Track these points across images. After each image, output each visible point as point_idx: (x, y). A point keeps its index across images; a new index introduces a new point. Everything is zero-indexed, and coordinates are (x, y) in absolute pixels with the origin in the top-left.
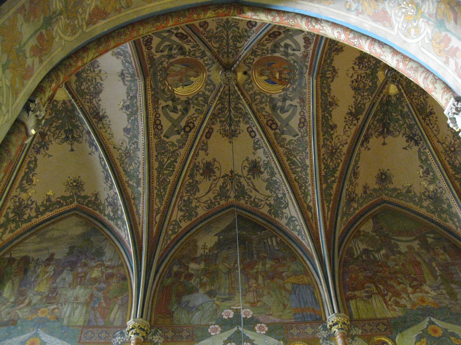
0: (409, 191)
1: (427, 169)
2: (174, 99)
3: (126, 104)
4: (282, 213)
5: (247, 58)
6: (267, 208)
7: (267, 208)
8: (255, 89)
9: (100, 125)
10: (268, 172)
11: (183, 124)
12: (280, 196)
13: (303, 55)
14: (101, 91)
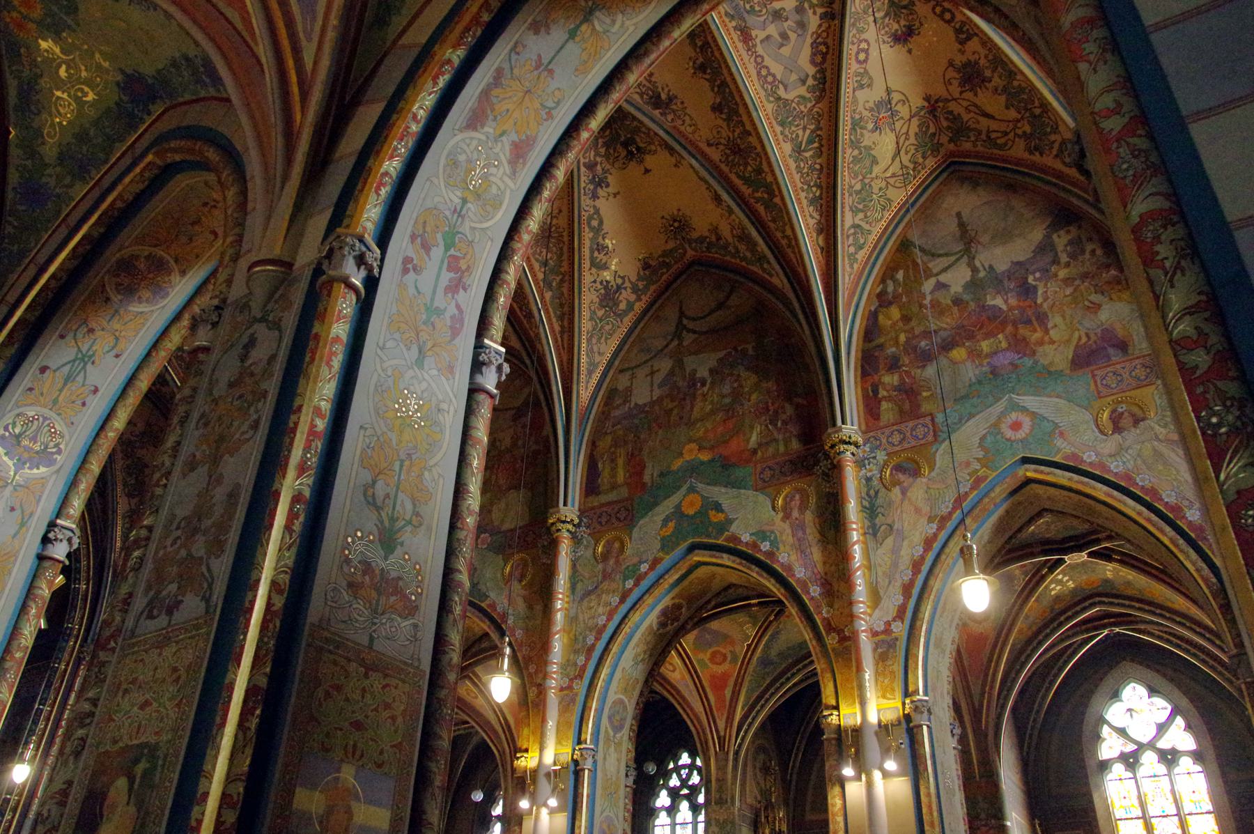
3: (698, 62)
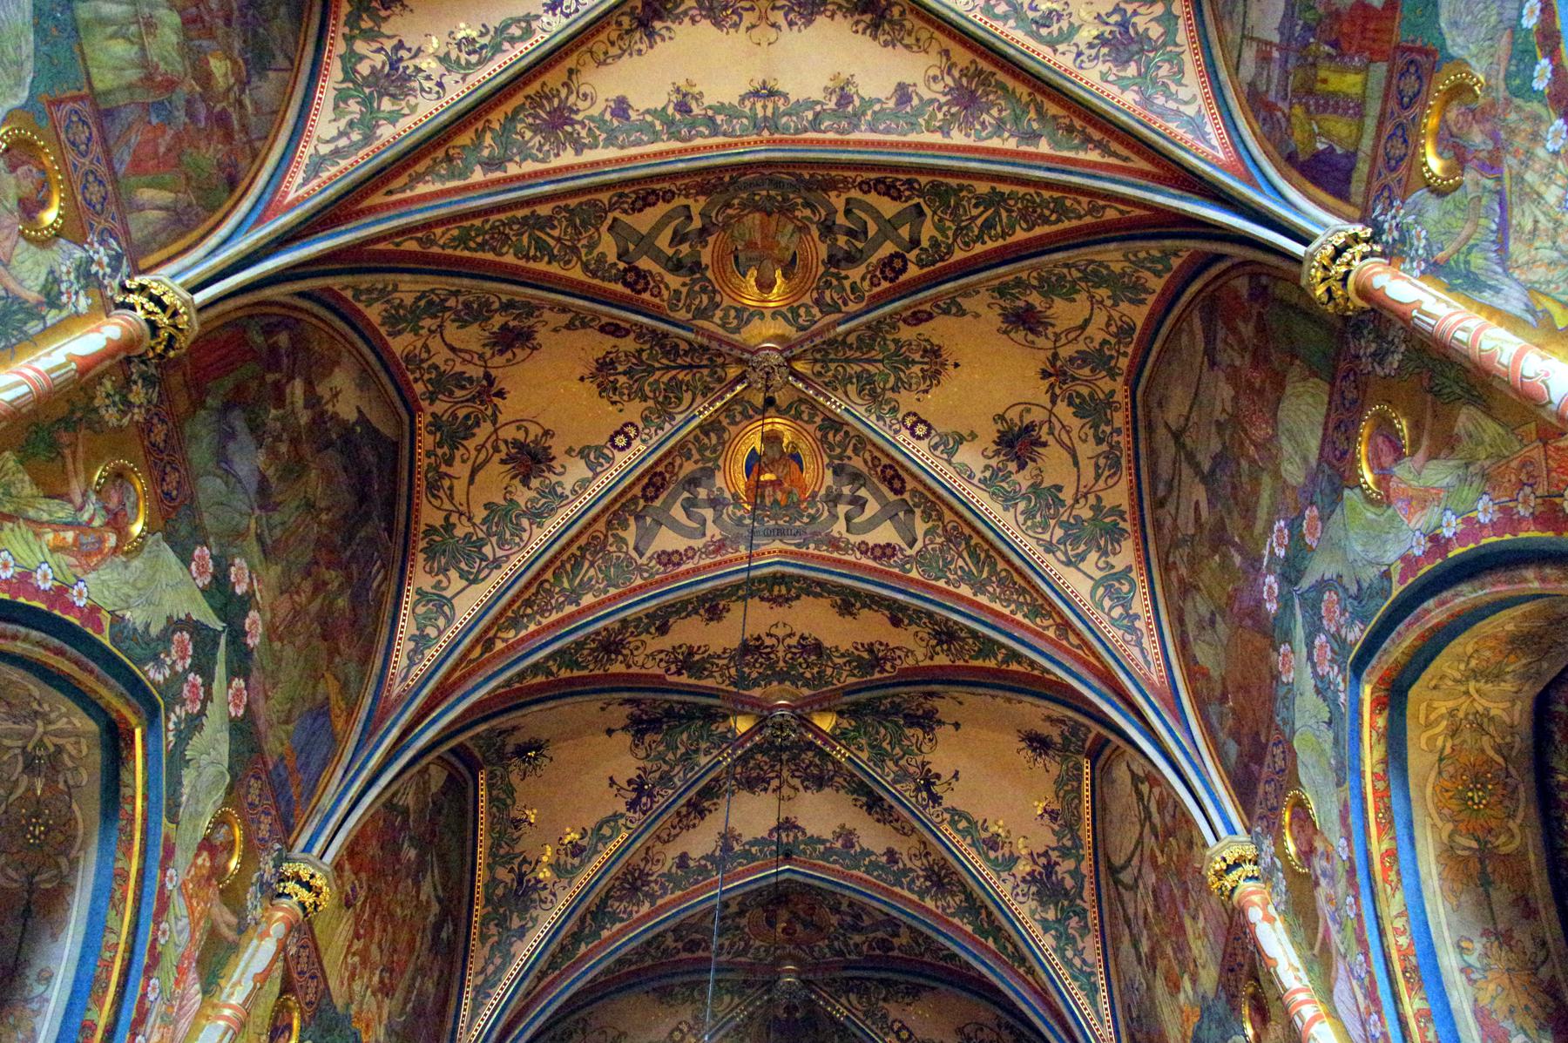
0: (517, 824)
1: (583, 849)
3: (694, 105)
4: (444, 570)
5: (813, 407)
6: (437, 519)
7: (437, 519)
8: (731, 428)
10: (532, 500)
11: (644, 263)
12: (487, 550)
13: (838, 540)
14: (718, 24)
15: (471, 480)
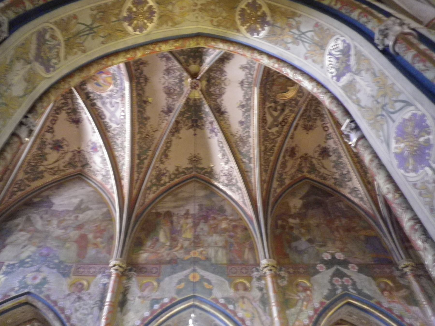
2: (275, 102)
9: (221, 118)
11: (280, 119)
14: (223, 94)
15: (325, 168)
